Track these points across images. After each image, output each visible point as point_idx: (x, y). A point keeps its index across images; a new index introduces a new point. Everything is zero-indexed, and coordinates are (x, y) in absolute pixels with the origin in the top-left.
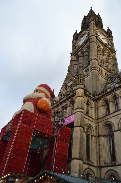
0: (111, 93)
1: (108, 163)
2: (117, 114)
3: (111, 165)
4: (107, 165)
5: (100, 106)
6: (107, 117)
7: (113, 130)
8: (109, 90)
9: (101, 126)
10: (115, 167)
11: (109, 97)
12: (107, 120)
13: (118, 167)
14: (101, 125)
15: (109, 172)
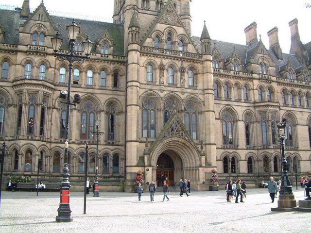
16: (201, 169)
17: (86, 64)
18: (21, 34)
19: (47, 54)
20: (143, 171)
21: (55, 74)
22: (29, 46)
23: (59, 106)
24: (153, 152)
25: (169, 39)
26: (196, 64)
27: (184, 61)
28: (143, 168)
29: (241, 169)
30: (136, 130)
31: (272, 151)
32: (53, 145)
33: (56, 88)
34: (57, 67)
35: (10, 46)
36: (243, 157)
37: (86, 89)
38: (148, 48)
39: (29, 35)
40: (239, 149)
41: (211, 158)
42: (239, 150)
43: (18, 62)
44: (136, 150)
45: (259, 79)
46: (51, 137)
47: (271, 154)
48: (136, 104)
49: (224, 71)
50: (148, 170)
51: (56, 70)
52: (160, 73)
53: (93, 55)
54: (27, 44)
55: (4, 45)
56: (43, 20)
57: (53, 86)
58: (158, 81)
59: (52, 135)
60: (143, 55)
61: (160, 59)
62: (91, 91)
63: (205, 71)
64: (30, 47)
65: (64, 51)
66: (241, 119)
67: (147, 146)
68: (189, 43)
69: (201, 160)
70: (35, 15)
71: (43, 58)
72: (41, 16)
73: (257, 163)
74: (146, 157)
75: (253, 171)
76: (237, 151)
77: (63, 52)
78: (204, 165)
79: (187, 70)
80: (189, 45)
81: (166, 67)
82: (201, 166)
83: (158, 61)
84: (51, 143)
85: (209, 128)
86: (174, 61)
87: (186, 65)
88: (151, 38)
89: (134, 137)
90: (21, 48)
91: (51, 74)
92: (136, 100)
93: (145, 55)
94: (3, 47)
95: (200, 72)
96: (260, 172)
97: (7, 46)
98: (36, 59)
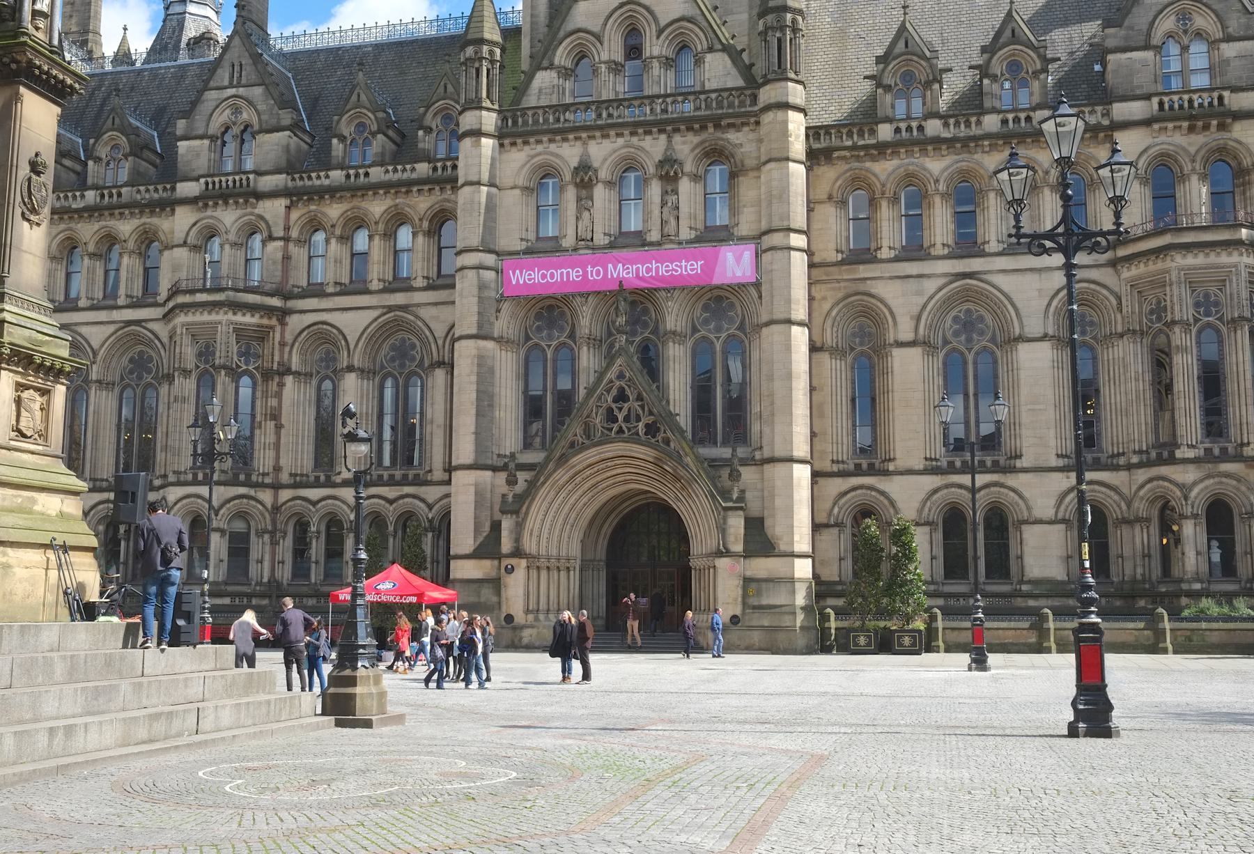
0: (895, 153)
1: (843, 462)
2: (915, 272)
3: (852, 467)
4: (841, 466)
5: (824, 196)
6: (863, 271)
7: (891, 338)
8: (885, 132)
9: (827, 306)
10: (883, 478)
11: (884, 169)
12: (861, 287)
13: (897, 478)
14: (824, 298)
15: (853, 494)
16: (723, 563)
17: (383, 208)
18: (183, 145)
19: (260, 196)
20: (493, 574)
21: (287, 258)
22: (202, 180)
23: (304, 362)
24: (533, 499)
25: (634, 50)
26: (732, 136)
27: (677, 130)
28: (496, 562)
29: (1029, 561)
30: (473, 429)
31: (1186, 475)
32: (285, 495)
33: (292, 304)
34: (294, 233)
35: (156, 190)
36: (1044, 506)
37: (386, 296)
38: (530, 113)
39: (206, 142)
40: (1025, 470)
41: (773, 516)
42: (1023, 477)
43: (179, 237)
44: (472, 498)
45: (1147, 123)
46: (277, 469)
47: (1181, 487)
48: (474, 331)
49: (946, 125)
50: (510, 570)
51: (291, 245)
52: (579, 199)
53: (395, 170)
54: (196, 174)
55: (139, 192)
56: (244, 81)
57: (275, 302)
58: (571, 232)
59: (283, 462)
60: (514, 144)
61: (578, 143)
62: (399, 298)
63: (763, 159)
64: (207, 184)
65: (314, 175)
66: (1034, 326)
67: (512, 482)
68: (711, 49)
69: (722, 530)
70: (219, 71)
71: (249, 210)
72: (237, 68)
73: (1126, 530)
74: (507, 524)
75: (1113, 569)
76: (1012, 480)
77: (310, 178)
78: (738, 547)
79: (688, 167)
80: (709, 57)
81: (604, 174)
82: (723, 552)
83: (569, 153)
84: (276, 487)
85: (771, 395)
86: (635, 140)
87: (685, 146)
88: (551, 67)
89: (465, 450)
90: (187, 189)
91: (274, 263)
92: (475, 318)
93: (519, 141)
94: (139, 197)
95: (750, 163)
96: (1139, 577)
97: (147, 191)
98: (229, 217)
